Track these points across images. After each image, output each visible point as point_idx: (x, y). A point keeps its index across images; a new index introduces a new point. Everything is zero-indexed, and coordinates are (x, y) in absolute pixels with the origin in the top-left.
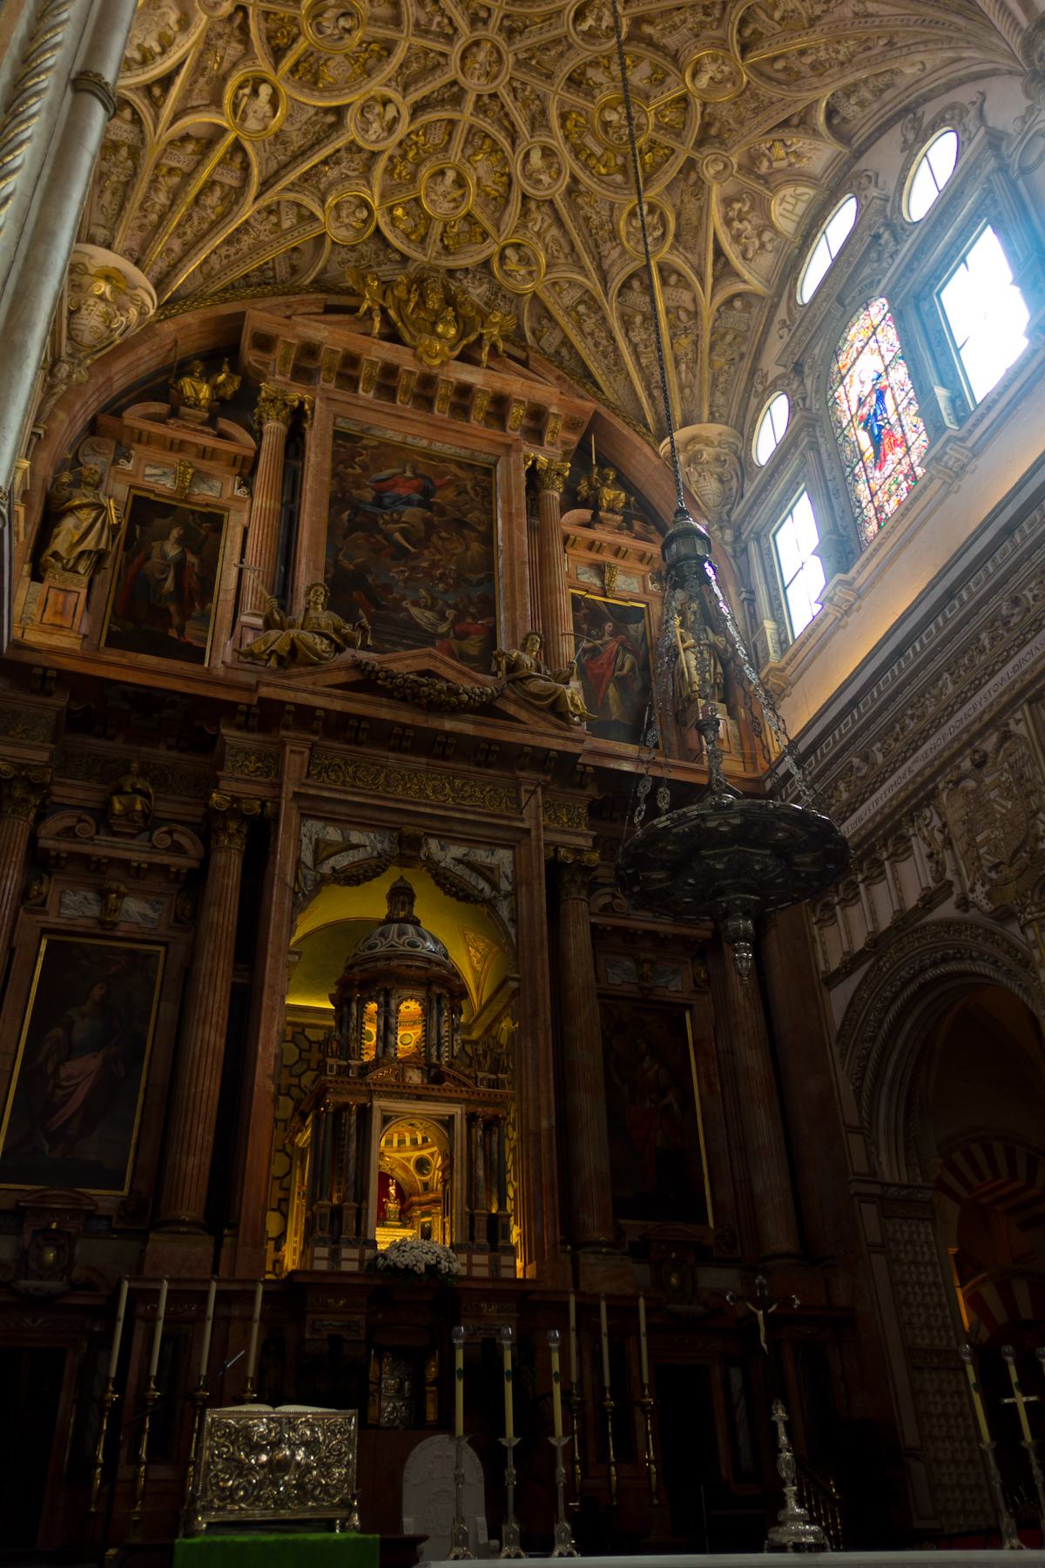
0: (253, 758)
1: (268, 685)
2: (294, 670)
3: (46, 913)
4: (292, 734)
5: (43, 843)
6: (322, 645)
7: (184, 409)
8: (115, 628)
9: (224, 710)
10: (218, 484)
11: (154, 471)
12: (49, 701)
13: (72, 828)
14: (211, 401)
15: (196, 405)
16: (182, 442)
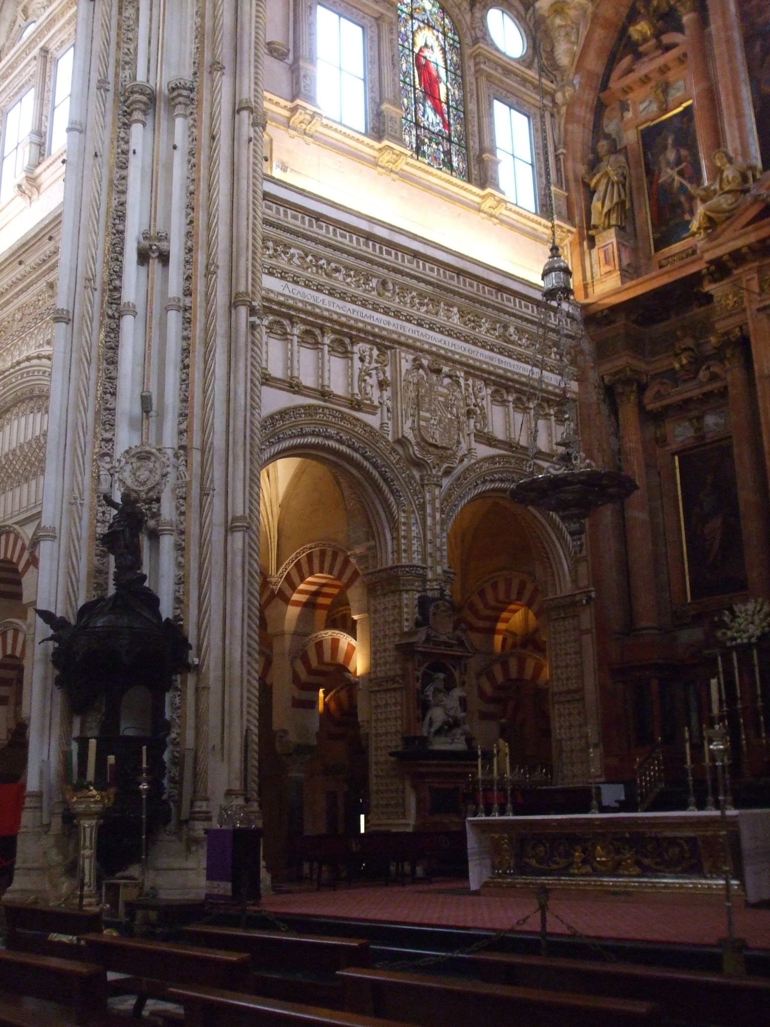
0: (731, 297)
1: (707, 250)
2: (719, 229)
3: (669, 445)
4: (739, 271)
5: (649, 407)
6: (724, 202)
7: (641, 49)
8: (658, 235)
9: (696, 279)
10: (681, 83)
11: (644, 105)
12: (617, 324)
13: (659, 392)
14: (654, 26)
15: (645, 40)
16: (646, 76)
